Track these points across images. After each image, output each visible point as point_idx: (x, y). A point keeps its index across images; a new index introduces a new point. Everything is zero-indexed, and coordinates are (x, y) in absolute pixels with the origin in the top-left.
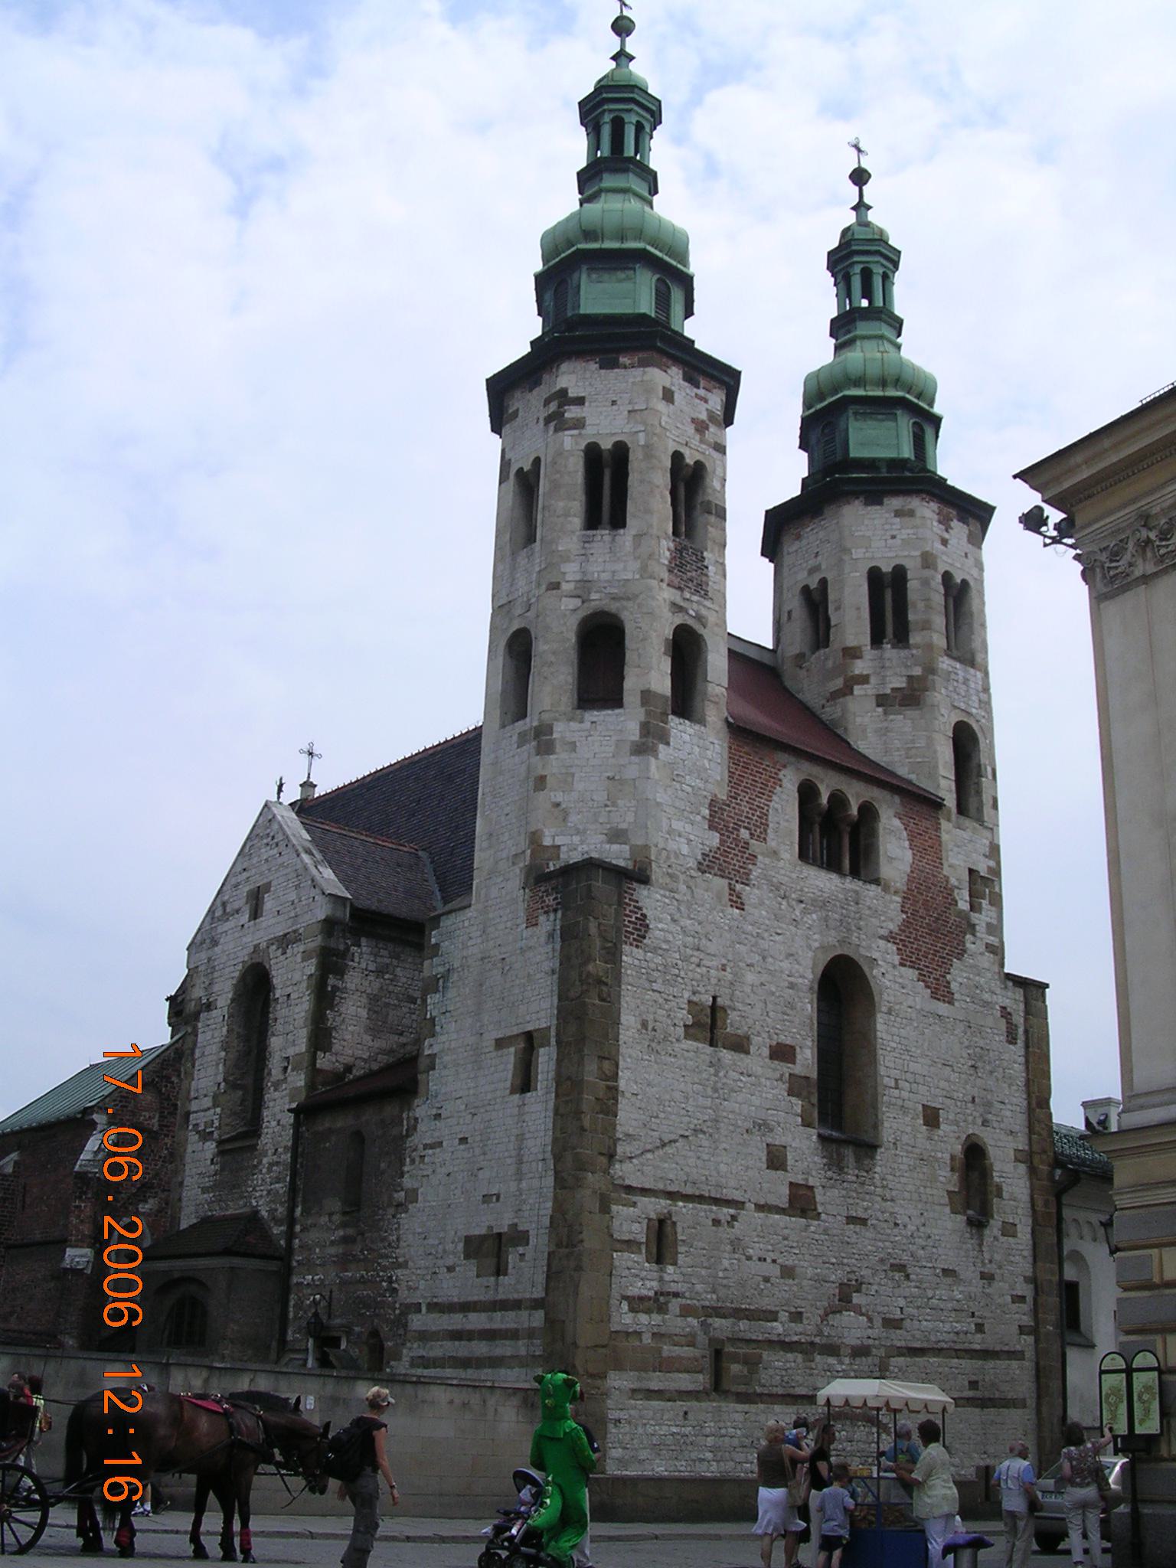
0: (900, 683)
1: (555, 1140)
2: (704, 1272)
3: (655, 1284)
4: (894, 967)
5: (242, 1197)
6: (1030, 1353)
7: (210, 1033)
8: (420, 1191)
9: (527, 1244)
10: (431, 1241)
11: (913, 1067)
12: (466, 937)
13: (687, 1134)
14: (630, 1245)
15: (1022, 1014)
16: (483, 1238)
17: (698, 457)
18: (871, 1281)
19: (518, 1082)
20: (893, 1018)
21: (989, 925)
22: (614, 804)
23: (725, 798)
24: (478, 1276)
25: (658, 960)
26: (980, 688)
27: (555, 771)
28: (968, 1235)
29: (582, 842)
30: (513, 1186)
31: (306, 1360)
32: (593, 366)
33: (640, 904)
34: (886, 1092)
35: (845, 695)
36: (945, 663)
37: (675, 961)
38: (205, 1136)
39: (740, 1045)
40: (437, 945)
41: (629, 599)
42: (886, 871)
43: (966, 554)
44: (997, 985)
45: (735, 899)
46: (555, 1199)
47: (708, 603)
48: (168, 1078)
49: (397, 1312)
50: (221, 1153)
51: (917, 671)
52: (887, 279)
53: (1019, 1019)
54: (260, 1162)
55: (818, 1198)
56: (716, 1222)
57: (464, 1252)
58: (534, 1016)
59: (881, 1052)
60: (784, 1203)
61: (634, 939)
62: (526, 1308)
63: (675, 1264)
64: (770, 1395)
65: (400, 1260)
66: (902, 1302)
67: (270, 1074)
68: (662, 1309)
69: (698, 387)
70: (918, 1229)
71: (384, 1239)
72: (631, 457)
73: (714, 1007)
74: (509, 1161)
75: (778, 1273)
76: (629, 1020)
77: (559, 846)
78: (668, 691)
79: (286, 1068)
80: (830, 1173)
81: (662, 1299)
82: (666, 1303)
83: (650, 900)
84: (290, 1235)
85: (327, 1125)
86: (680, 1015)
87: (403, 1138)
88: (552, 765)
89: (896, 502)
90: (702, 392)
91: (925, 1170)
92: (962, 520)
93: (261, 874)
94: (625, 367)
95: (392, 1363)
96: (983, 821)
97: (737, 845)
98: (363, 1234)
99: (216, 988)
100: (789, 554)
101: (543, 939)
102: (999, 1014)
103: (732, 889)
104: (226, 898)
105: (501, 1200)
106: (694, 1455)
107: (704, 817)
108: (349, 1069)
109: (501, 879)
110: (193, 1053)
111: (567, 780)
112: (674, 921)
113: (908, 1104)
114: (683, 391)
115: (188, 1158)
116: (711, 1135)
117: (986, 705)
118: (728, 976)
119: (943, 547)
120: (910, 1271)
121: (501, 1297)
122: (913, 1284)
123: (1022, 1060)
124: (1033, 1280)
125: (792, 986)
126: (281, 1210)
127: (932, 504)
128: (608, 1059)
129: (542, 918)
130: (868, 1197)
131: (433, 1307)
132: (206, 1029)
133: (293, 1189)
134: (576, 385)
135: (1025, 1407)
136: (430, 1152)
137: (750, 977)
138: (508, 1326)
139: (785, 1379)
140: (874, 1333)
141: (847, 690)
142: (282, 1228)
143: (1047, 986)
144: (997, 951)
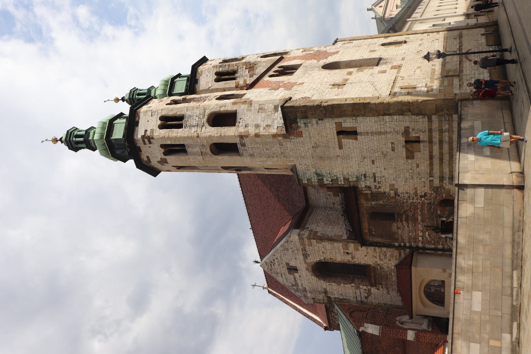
0: (247, 71)
1: (373, 116)
5: (391, 274)
7: (335, 291)
9: (408, 127)
10: (408, 176)
12: (306, 166)
16: (407, 150)
19: (354, 136)
24: (420, 151)
29: (277, 119)
30: (389, 136)
38: (369, 293)
39: (347, 80)
40: (308, 180)
41: (205, 112)
42: (300, 63)
49: (433, 192)
51: (244, 67)
54: (379, 265)
57: (412, 159)
58: (332, 131)
60: (396, 70)
62: (431, 126)
65: (414, 191)
74: (380, 138)
75: (419, 70)
76: (336, 97)
79: (348, 253)
81: (428, 86)
87: (372, 194)
93: (283, 268)
98: (405, 211)
99: (320, 289)
105: (393, 141)
109: (287, 150)
110: (341, 299)
111: (257, 126)
113: (368, 54)
121: (427, 140)
126: (396, 253)
129: (300, 130)
132: (333, 293)
136: (377, 179)
137: (326, 80)
138: (438, 135)
142: (402, 253)
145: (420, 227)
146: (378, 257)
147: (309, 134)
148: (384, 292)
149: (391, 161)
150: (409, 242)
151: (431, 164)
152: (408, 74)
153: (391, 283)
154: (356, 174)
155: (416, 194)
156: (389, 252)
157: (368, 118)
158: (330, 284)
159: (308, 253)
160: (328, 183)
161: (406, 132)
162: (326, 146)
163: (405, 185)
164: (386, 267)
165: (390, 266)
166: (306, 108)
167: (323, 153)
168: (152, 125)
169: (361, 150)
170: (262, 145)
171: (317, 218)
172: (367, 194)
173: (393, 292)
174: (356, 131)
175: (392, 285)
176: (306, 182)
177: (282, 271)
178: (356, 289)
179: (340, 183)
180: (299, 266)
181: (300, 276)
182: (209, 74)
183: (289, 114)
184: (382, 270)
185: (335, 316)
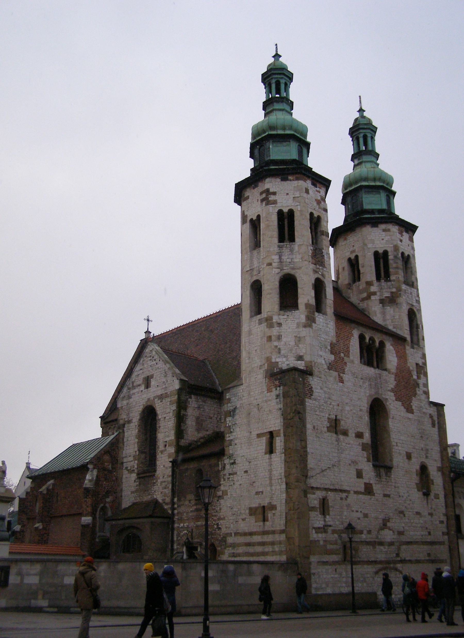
0: (388, 295)
1: (285, 472)
2: (338, 517)
3: (323, 523)
4: (393, 401)
5: (149, 495)
6: (447, 543)
8: (229, 491)
9: (276, 509)
10: (234, 510)
11: (402, 438)
13: (330, 467)
14: (313, 509)
15: (436, 416)
16: (256, 508)
17: (319, 214)
18: (393, 517)
19: (268, 450)
20: (394, 420)
21: (424, 384)
22: (298, 346)
23: (335, 342)
24: (256, 522)
25: (317, 403)
26: (416, 295)
27: (275, 334)
28: (423, 499)
29: (287, 360)
30: (269, 488)
31: (183, 556)
32: (278, 180)
33: (310, 383)
34: (394, 448)
35: (367, 299)
36: (404, 287)
37: (323, 403)
38: (131, 471)
39: (345, 433)
41: (298, 269)
43: (408, 245)
44: (427, 406)
45: (340, 379)
46: (287, 492)
47: (325, 269)
48: (114, 450)
49: (222, 536)
50: (139, 478)
51: (394, 290)
52: (373, 138)
53: (435, 418)
54: (157, 481)
55: (374, 488)
56: (341, 499)
57: (249, 513)
58: (273, 426)
59: (391, 433)
60: (363, 490)
61: (309, 396)
62: (277, 533)
63: (329, 514)
64: (362, 561)
65: (222, 517)
66: (403, 525)
67: (158, 448)
68: (326, 532)
69: (316, 187)
70: (407, 498)
71: (214, 509)
72: (295, 215)
73: (336, 420)
77: (278, 362)
78: (314, 304)
79: (166, 446)
80: (377, 479)
81: (326, 528)
82: (327, 529)
83: (314, 382)
84: (173, 509)
85: (186, 467)
86: (325, 423)
87: (219, 471)
88: (275, 331)
89: (383, 226)
90: (318, 189)
91: (408, 476)
92: (407, 232)
93: (149, 371)
94: (291, 180)
95: (221, 556)
96: (420, 345)
97: (340, 359)
99: (131, 415)
100: (342, 245)
101: (275, 397)
102: (428, 416)
103: (339, 375)
104: (134, 380)
105: (264, 493)
106: (339, 585)
107: (329, 350)
108: (190, 444)
109: (255, 374)
110: (123, 440)
111: (279, 338)
112: (321, 389)
113: (401, 451)
114: (312, 189)
115: (124, 480)
116: (338, 467)
117: (418, 302)
118: (340, 408)
119: (401, 243)
120: (405, 513)
122: (406, 518)
123: (437, 433)
124: (446, 515)
125: (361, 410)
126: (168, 500)
127: (396, 227)
128: (304, 441)
129: (274, 389)
130: (390, 487)
131: (236, 534)
133: (173, 491)
134: (272, 187)
135: (446, 562)
136: (232, 476)
137: (347, 408)
139: (367, 555)
140: (395, 537)
141: (368, 298)
142: (168, 506)
143: (444, 405)
144: (427, 393)
145: (192, 524)
146: (164, 480)
147: (270, 400)
148: (133, 488)
149: (247, 491)
150: (178, 513)
151: (245, 534)
152: (352, 504)
153: (141, 495)
154: (236, 453)
155: (220, 519)
156: (168, 491)
157: (283, 466)
158: (137, 426)
159: (164, 401)
160: (227, 422)
161: (273, 507)
162: (259, 419)
163: (227, 507)
164: (155, 489)
165: (156, 493)
166: (292, 397)
167: (253, 416)
168: (282, 201)
169: (256, 458)
170: (260, 344)
171: (205, 406)
172: (218, 466)
173: (133, 498)
174: (273, 453)
175: (139, 496)
176: (227, 397)
177: (145, 370)
178: (134, 456)
179: (227, 435)
180: (152, 389)
181: (142, 391)
182: (384, 241)
183: (287, 377)
184: (152, 484)
185: (116, 429)
